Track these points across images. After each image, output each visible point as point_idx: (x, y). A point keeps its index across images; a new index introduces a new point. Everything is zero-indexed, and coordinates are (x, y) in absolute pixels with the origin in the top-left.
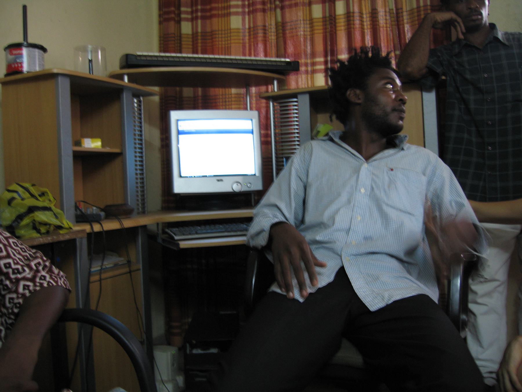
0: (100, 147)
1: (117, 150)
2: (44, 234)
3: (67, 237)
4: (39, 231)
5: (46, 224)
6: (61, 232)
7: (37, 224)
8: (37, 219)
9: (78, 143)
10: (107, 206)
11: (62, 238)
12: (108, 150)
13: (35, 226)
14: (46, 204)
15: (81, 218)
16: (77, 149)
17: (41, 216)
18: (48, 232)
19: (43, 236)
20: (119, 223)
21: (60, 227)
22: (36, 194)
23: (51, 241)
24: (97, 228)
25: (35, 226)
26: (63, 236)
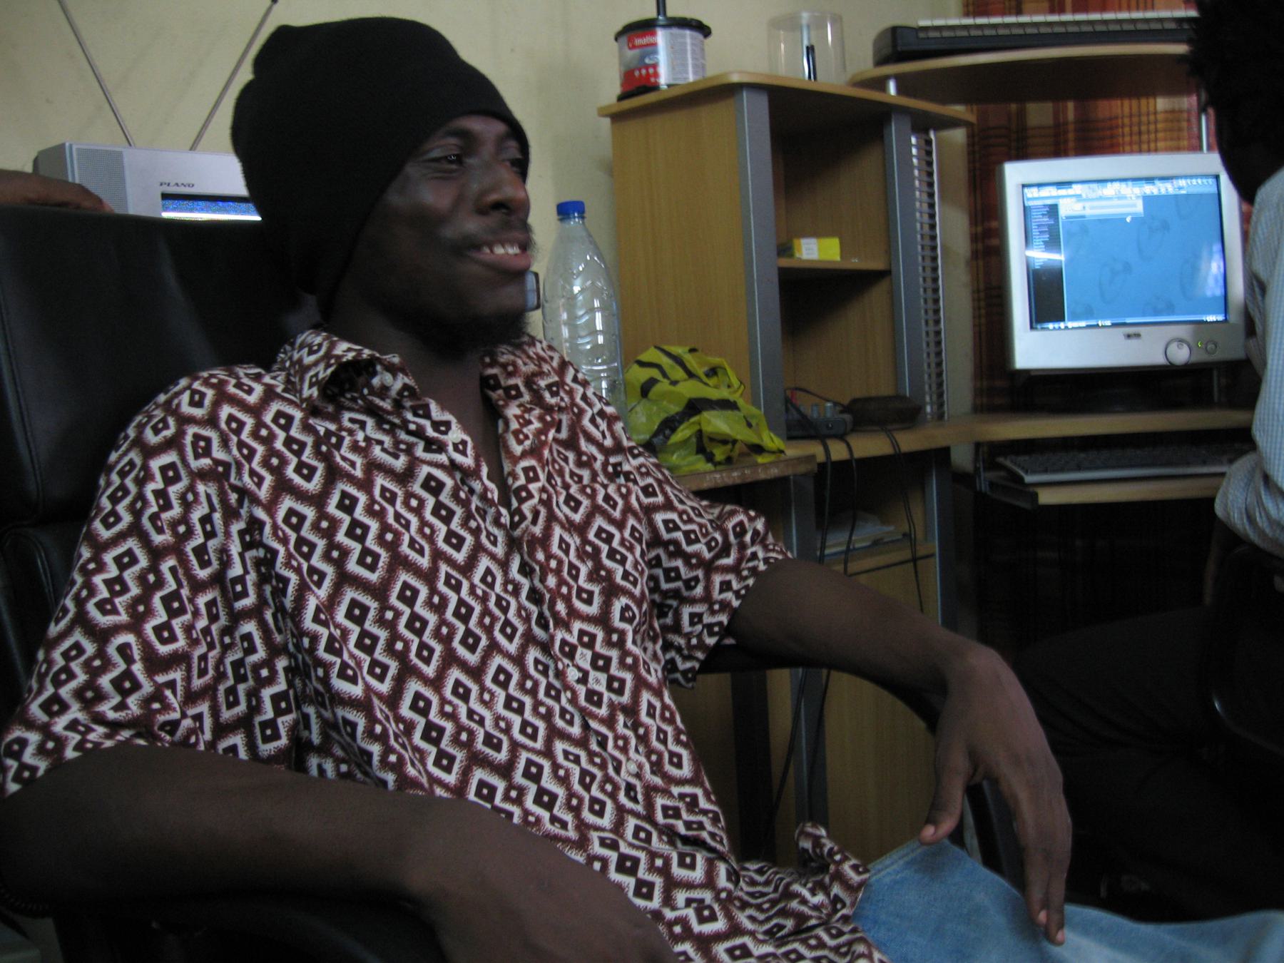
0: (838, 258)
1: (876, 264)
2: (720, 463)
3: (774, 472)
4: (710, 458)
5: (724, 441)
6: (761, 460)
7: (705, 440)
8: (707, 429)
9: (785, 249)
10: (855, 401)
11: (762, 475)
12: (855, 263)
13: (703, 444)
14: (724, 393)
15: (800, 429)
16: (785, 262)
17: (715, 422)
18: (729, 460)
19: (719, 468)
20: (888, 440)
21: (758, 449)
22: (700, 371)
23: (738, 481)
24: (838, 451)
25: (703, 444)
26: (764, 469)
